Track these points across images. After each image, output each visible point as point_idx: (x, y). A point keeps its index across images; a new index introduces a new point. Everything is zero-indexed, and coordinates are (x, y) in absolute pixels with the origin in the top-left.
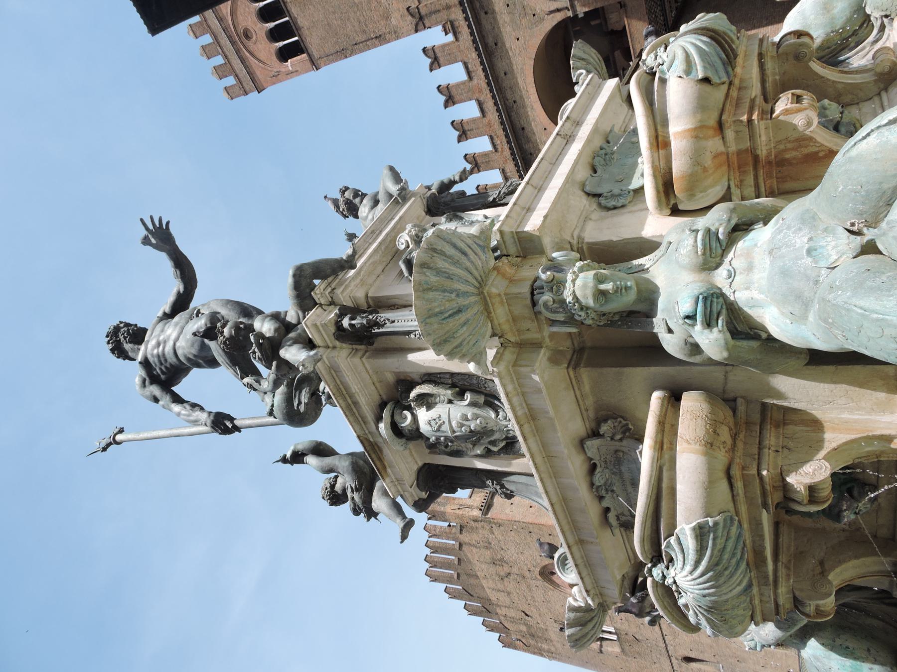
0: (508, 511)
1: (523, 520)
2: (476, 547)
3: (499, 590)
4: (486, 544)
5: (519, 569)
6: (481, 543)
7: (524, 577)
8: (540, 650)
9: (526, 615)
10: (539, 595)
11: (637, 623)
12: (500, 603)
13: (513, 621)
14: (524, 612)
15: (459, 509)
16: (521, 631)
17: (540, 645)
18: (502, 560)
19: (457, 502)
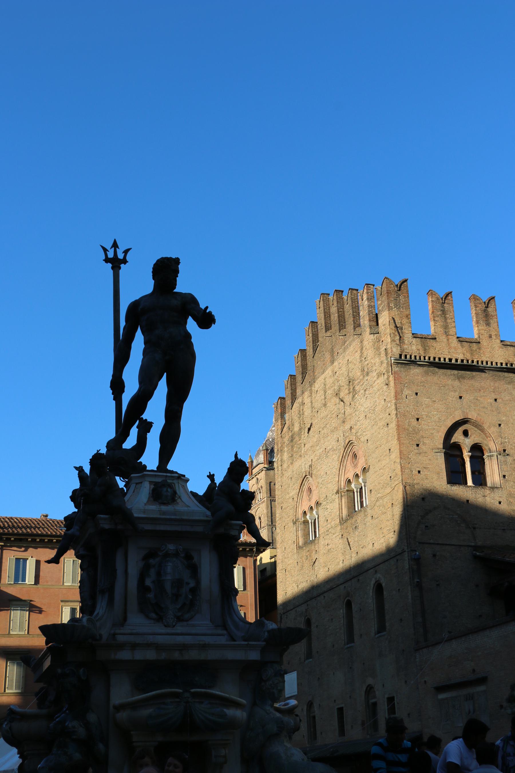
0: (406, 392)
1: (398, 413)
2: (361, 356)
3: (325, 392)
4: (366, 370)
5: (351, 414)
6: (367, 363)
7: (344, 422)
8: (281, 450)
9: (309, 429)
10: (331, 442)
11: (329, 563)
12: (314, 395)
13: (301, 414)
14: (311, 425)
15: (396, 327)
16: (293, 425)
17: (286, 448)
18: (354, 392)
19: (405, 321)
